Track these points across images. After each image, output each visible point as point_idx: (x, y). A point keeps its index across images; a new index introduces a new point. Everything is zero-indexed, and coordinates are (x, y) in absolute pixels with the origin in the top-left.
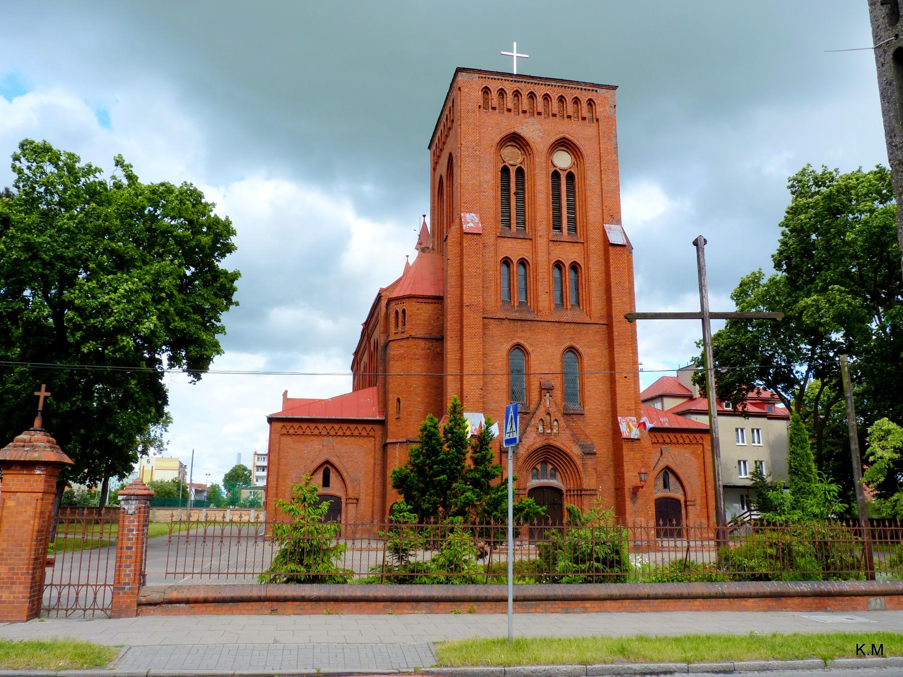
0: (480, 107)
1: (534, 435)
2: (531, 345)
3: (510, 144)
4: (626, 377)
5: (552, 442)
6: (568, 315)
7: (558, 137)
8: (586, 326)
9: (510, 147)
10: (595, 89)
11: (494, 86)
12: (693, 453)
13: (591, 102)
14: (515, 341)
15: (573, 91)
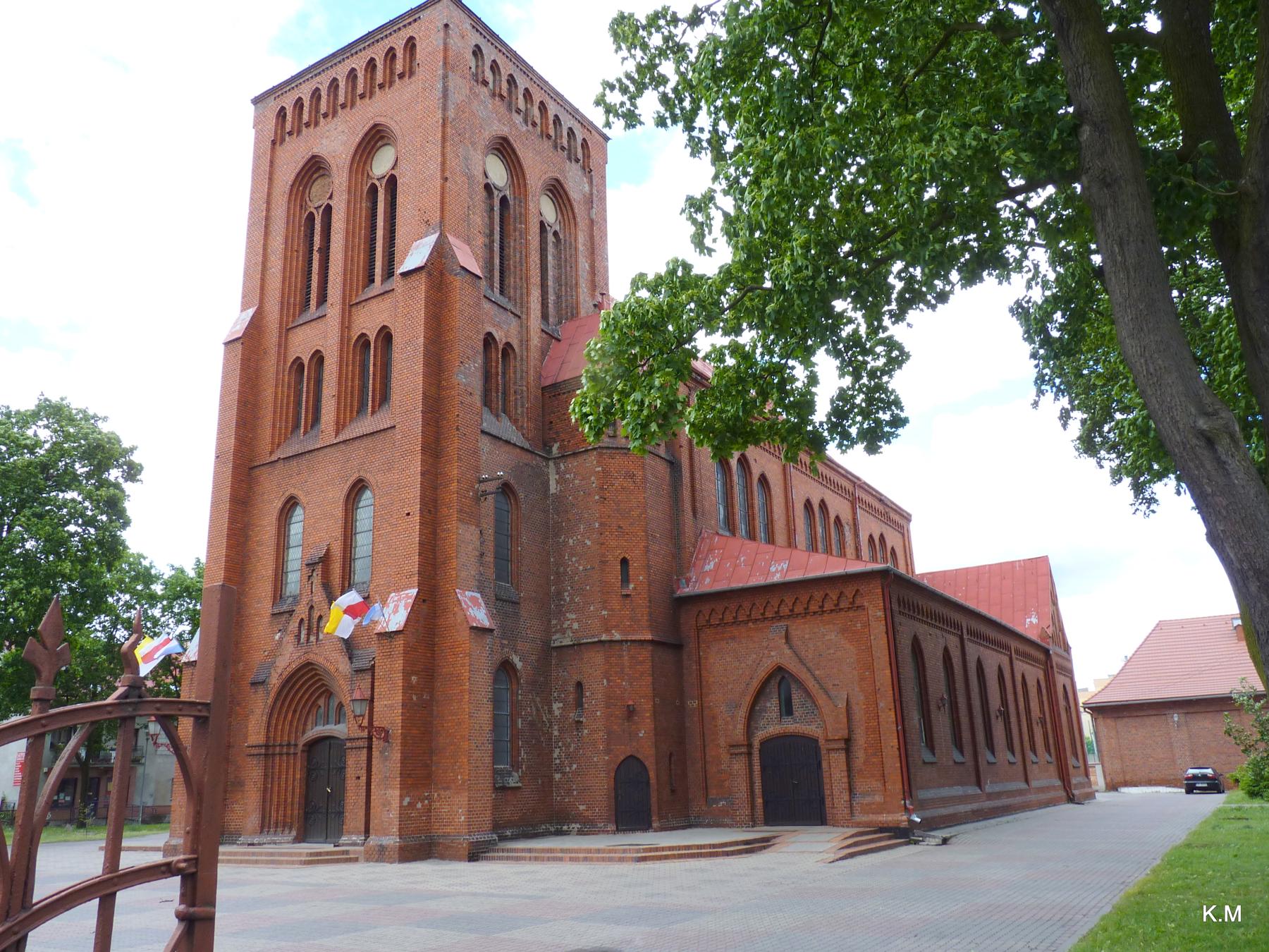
0: (274, 142)
1: (290, 648)
2: (307, 494)
3: (315, 176)
4: (408, 514)
5: (312, 657)
6: (367, 424)
7: (366, 128)
8: (382, 436)
9: (319, 181)
10: (417, 16)
11: (288, 102)
12: (844, 631)
13: (411, 44)
14: (287, 494)
15: (386, 41)
